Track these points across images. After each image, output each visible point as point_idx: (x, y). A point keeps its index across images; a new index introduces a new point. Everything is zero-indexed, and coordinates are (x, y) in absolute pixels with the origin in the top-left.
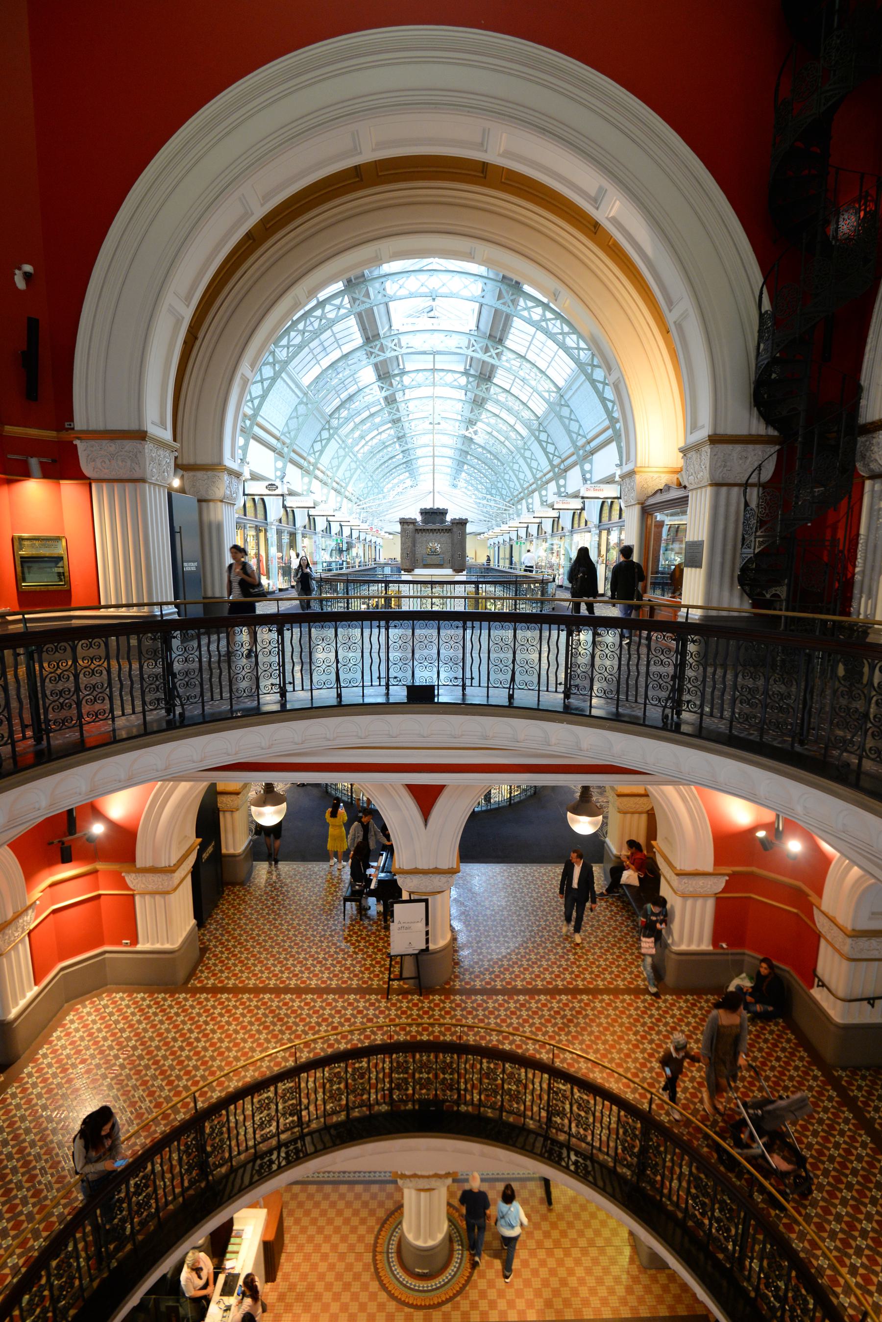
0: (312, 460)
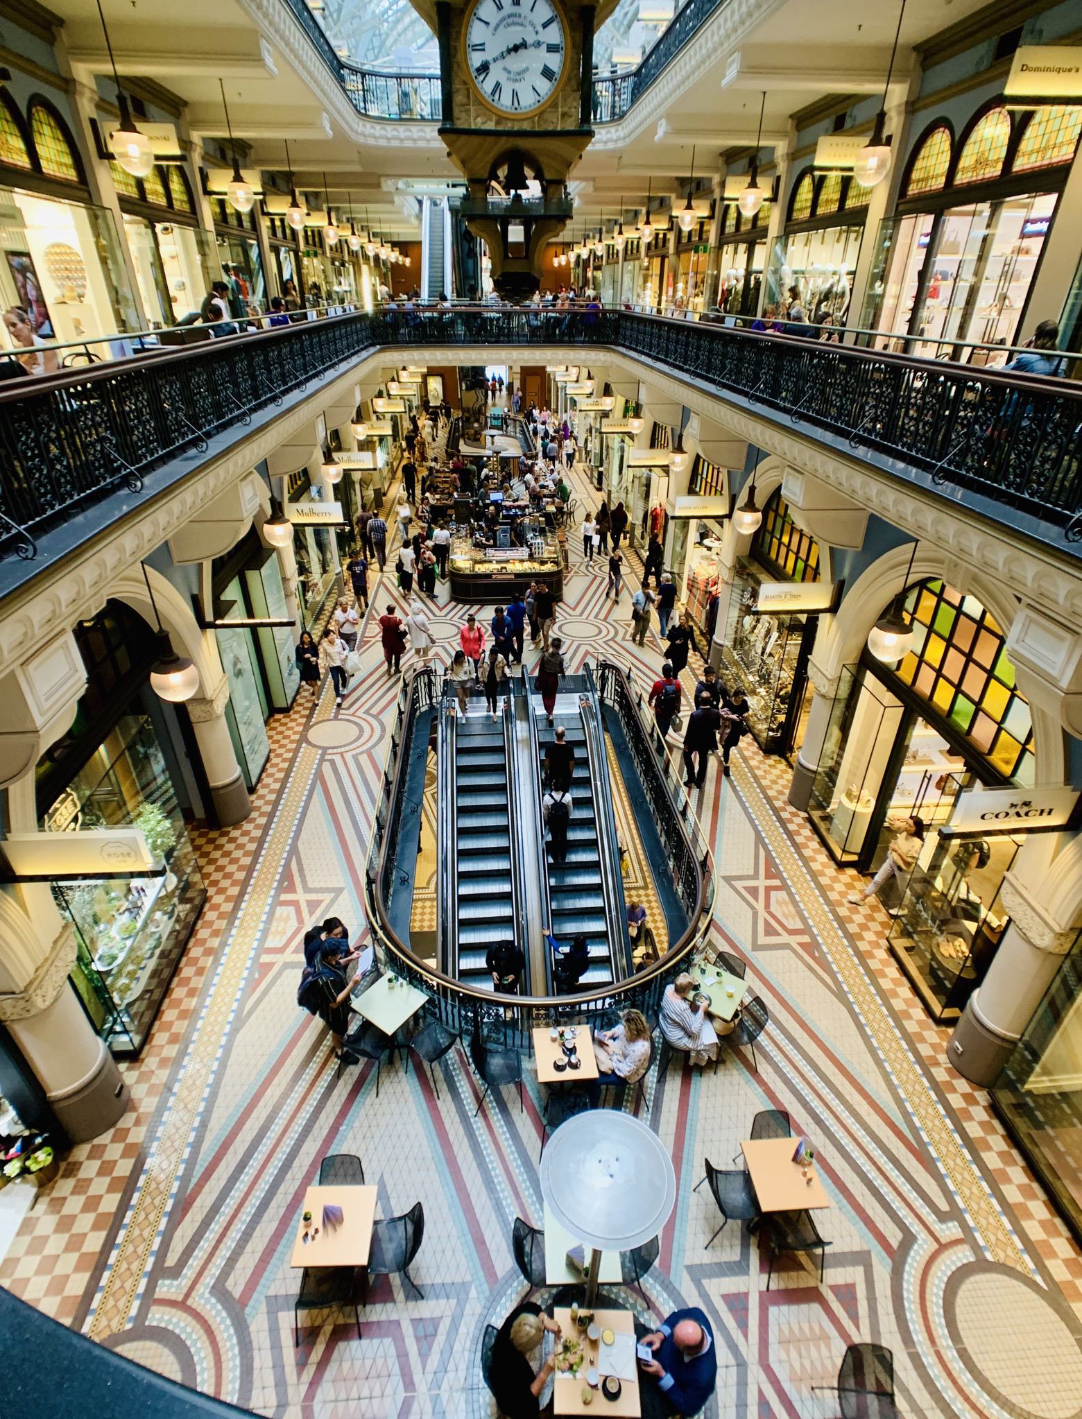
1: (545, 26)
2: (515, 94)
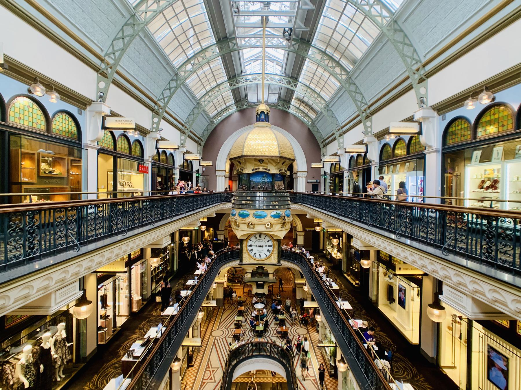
0: (162, 105)
1: (268, 242)
2: (260, 255)
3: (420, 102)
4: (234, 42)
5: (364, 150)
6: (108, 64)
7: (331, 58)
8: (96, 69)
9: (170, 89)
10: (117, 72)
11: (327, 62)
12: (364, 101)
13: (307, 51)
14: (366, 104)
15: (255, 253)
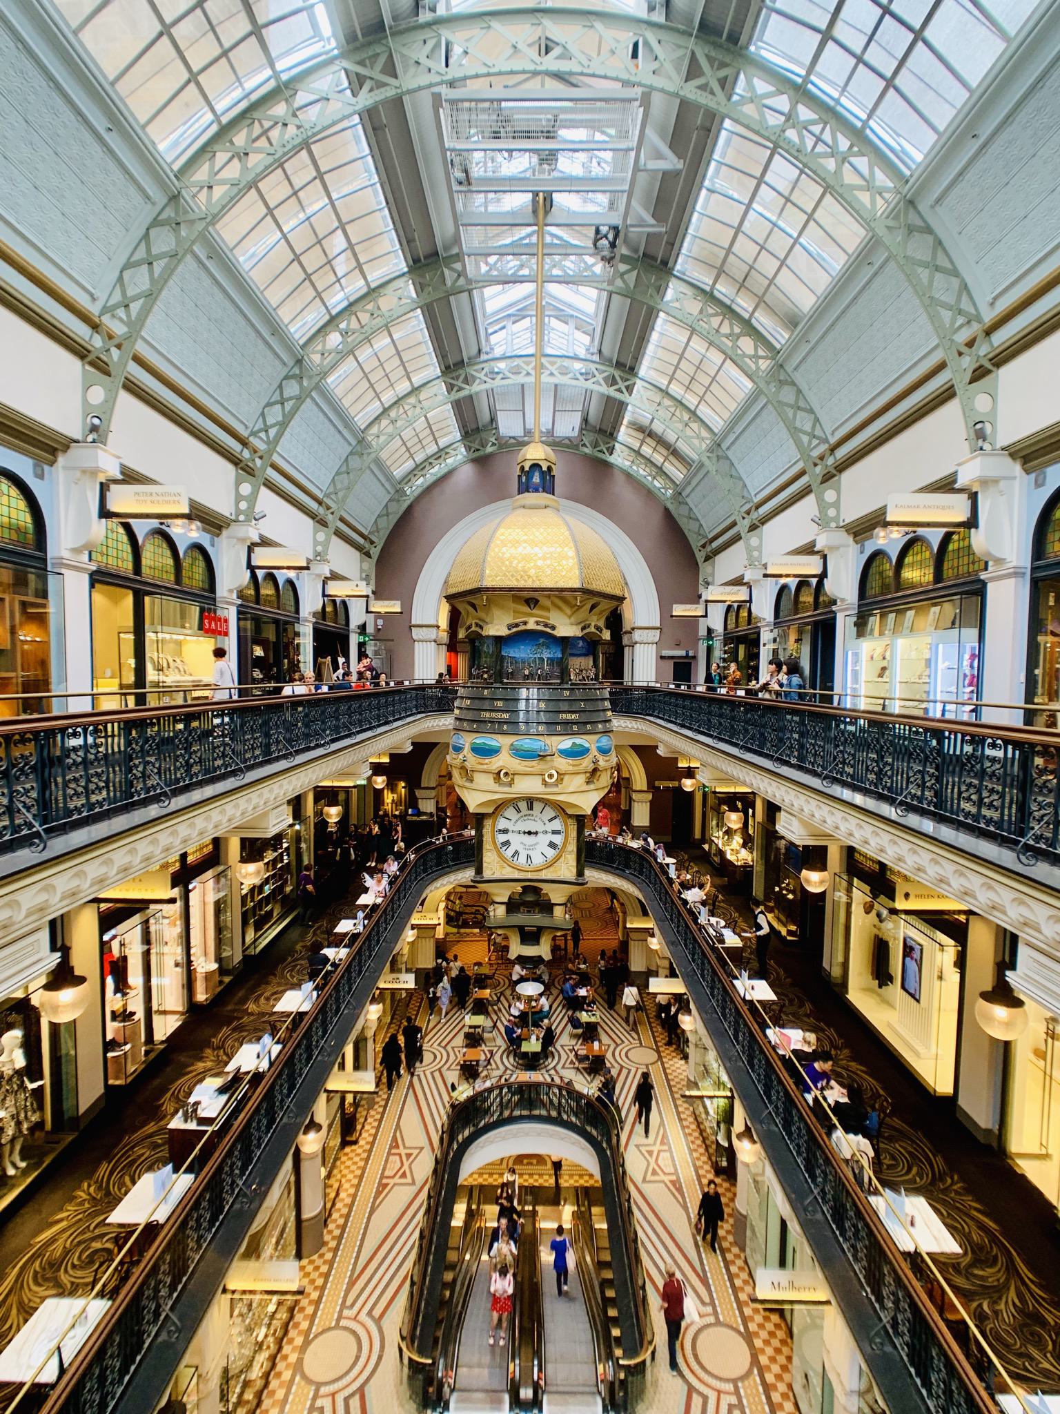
0: (261, 446)
2: (529, 857)
3: (973, 435)
4: (458, 266)
5: (818, 571)
6: (110, 337)
7: (729, 311)
8: (80, 351)
9: (283, 404)
10: (138, 360)
11: (716, 321)
12: (818, 432)
13: (660, 290)
14: (826, 441)
15: (516, 852)
